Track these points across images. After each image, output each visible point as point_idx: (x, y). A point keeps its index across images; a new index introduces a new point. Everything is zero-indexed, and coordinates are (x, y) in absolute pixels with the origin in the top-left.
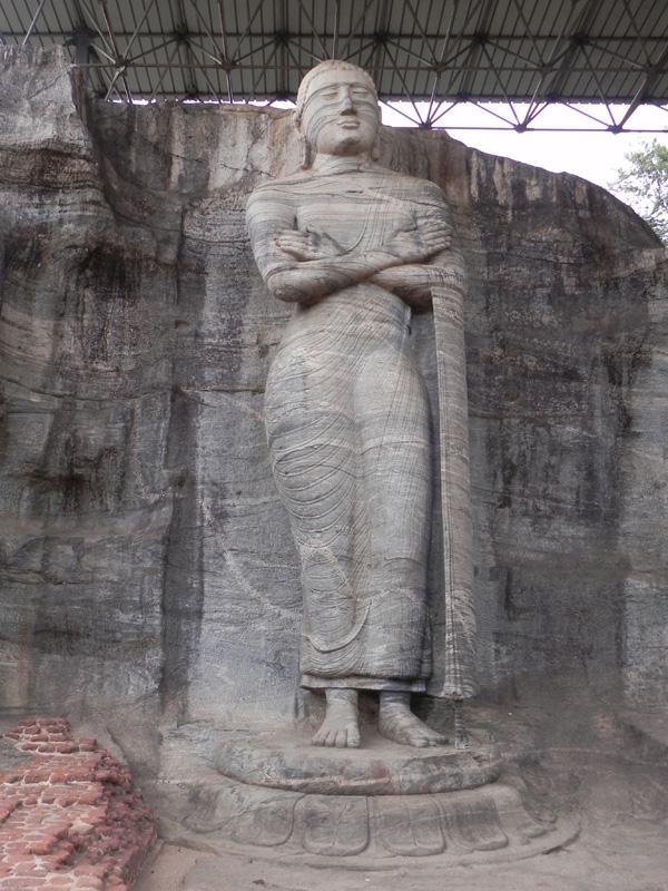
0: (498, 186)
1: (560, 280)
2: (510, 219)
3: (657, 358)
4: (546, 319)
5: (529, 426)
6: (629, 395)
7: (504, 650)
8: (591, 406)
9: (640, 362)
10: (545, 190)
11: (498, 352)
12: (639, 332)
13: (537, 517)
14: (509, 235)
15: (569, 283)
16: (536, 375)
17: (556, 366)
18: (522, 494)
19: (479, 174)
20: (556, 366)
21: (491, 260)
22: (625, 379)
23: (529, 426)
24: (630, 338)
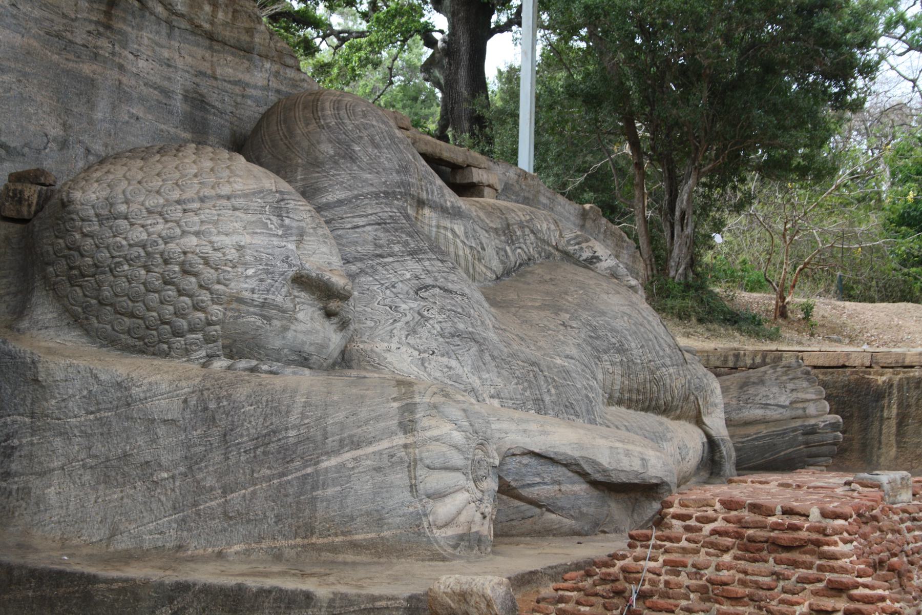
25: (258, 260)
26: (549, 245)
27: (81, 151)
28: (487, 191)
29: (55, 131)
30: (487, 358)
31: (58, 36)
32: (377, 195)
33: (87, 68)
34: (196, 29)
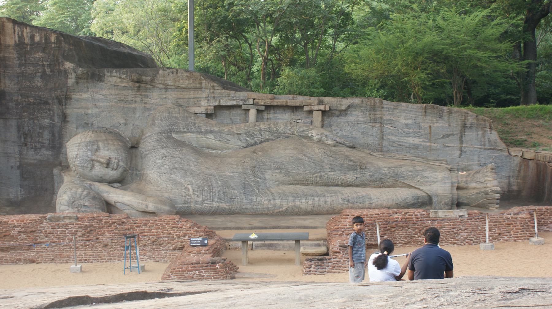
0: (25, 37)
1: (45, 70)
2: (29, 49)
3: (73, 96)
4: (39, 84)
5: (32, 121)
6: (66, 108)
7: (22, 190)
8: (54, 113)
9: (68, 98)
10: (41, 39)
11: (20, 98)
12: (65, 89)
13: (36, 149)
14: (25, 57)
15: (48, 71)
16: (34, 104)
17: (41, 100)
18: (31, 142)
19: (18, 33)
20: (41, 100)
21: (20, 65)
22: (64, 104)
23: (32, 121)
24: (61, 92)
25: (80, 157)
26: (284, 133)
27: (131, 125)
28: (314, 112)
29: (122, 121)
30: (188, 174)
31: (123, 100)
32: (158, 133)
33: (133, 106)
34: (178, 88)
